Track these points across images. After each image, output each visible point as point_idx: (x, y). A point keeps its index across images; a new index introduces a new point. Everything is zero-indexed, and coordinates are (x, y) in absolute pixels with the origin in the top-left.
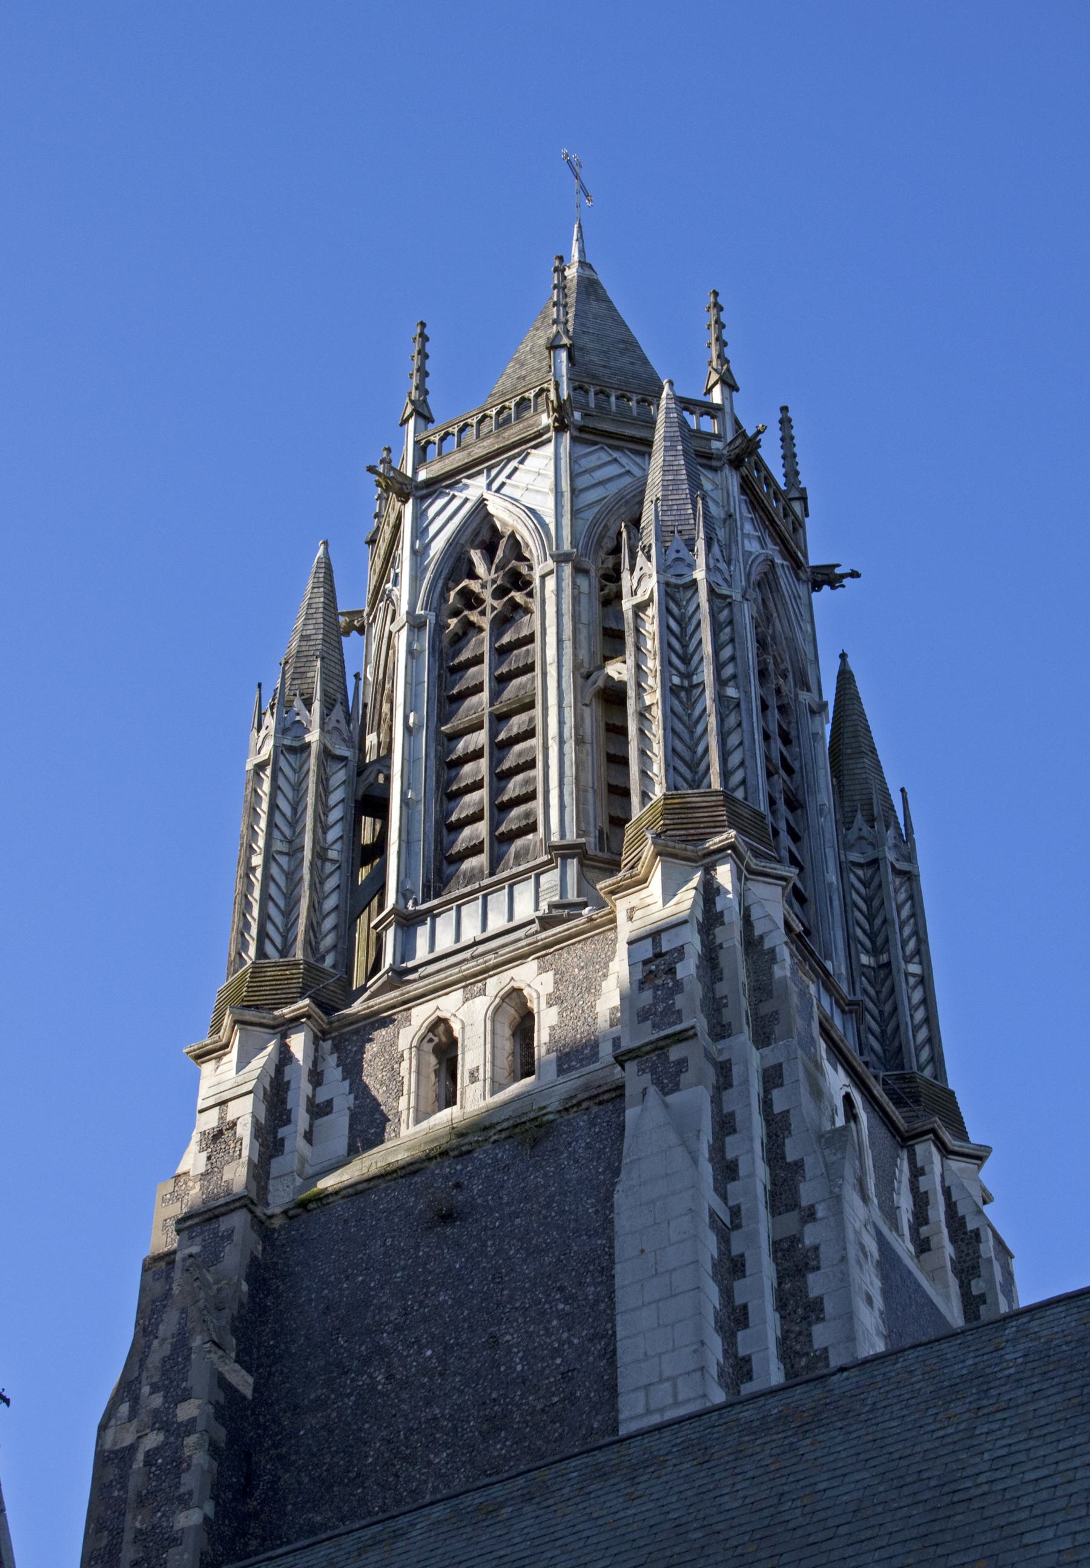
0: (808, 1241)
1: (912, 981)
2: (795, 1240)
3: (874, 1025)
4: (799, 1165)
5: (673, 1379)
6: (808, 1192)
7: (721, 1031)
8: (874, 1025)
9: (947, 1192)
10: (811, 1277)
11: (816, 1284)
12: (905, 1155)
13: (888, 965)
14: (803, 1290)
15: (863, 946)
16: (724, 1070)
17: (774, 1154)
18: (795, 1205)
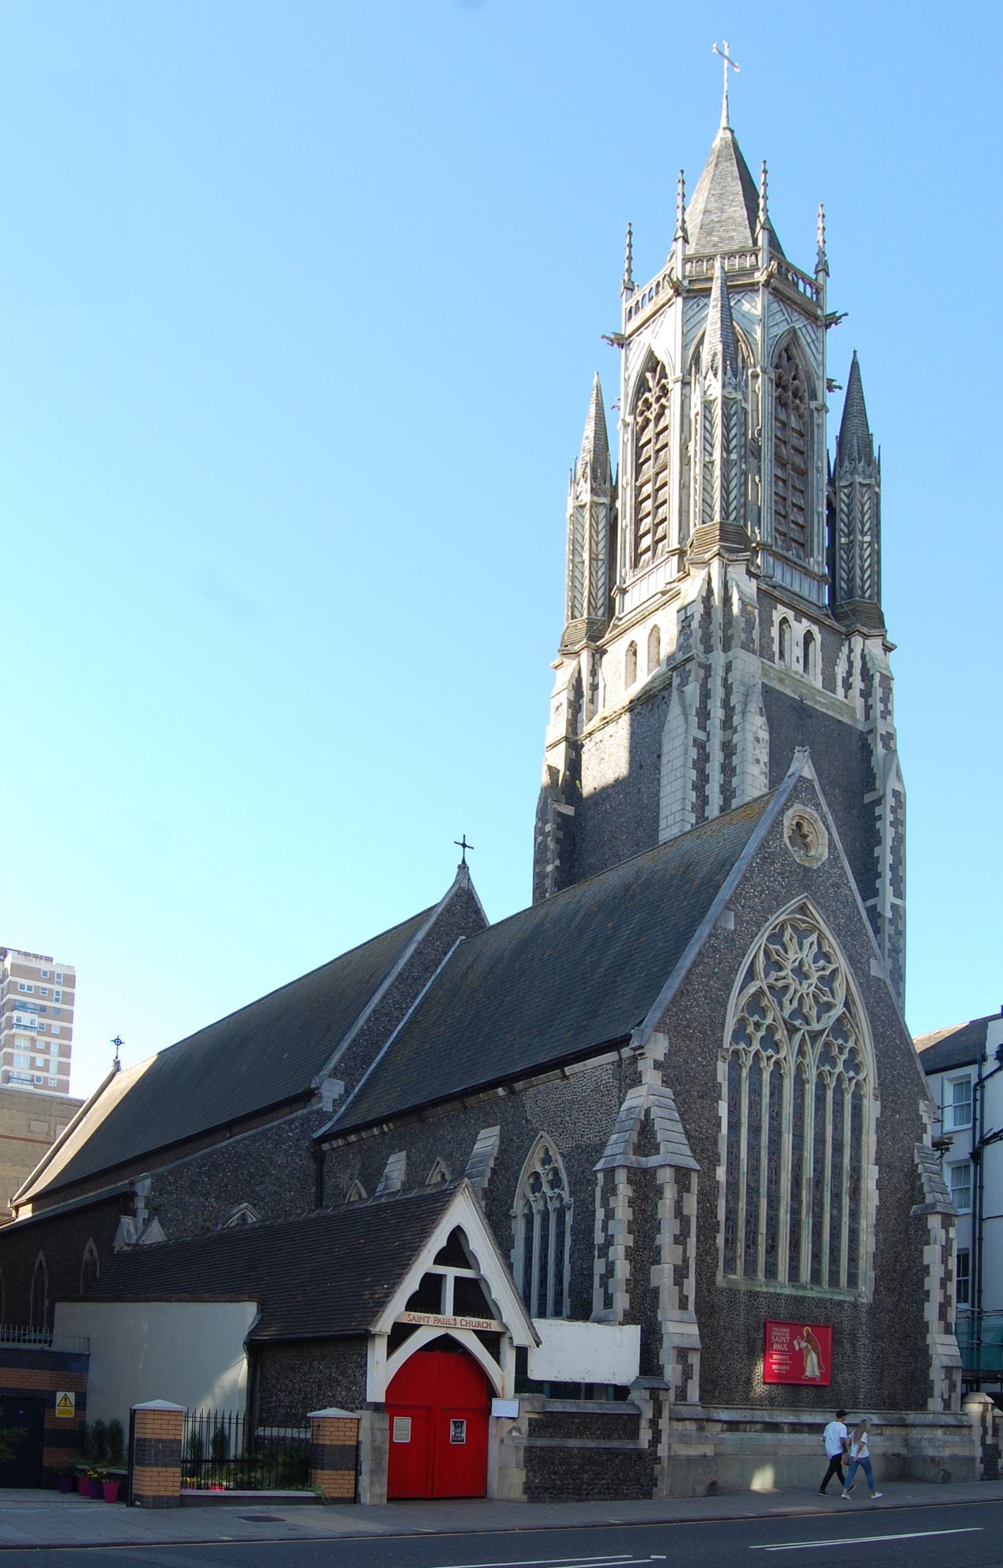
0: (734, 741)
1: (865, 545)
2: (730, 741)
3: (844, 575)
4: (734, 707)
5: (674, 814)
6: (736, 719)
7: (709, 649)
8: (844, 575)
9: (863, 657)
10: (734, 757)
11: (735, 760)
12: (847, 643)
13: (852, 541)
14: (731, 763)
15: (843, 532)
16: (708, 668)
17: (726, 704)
18: (731, 727)
